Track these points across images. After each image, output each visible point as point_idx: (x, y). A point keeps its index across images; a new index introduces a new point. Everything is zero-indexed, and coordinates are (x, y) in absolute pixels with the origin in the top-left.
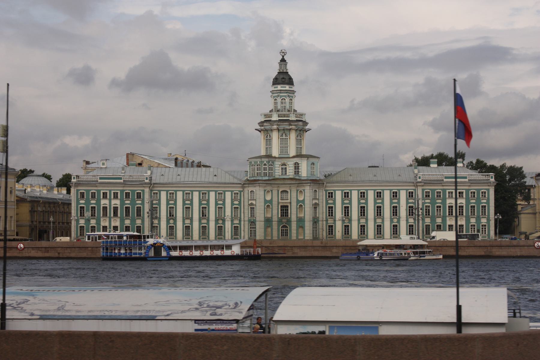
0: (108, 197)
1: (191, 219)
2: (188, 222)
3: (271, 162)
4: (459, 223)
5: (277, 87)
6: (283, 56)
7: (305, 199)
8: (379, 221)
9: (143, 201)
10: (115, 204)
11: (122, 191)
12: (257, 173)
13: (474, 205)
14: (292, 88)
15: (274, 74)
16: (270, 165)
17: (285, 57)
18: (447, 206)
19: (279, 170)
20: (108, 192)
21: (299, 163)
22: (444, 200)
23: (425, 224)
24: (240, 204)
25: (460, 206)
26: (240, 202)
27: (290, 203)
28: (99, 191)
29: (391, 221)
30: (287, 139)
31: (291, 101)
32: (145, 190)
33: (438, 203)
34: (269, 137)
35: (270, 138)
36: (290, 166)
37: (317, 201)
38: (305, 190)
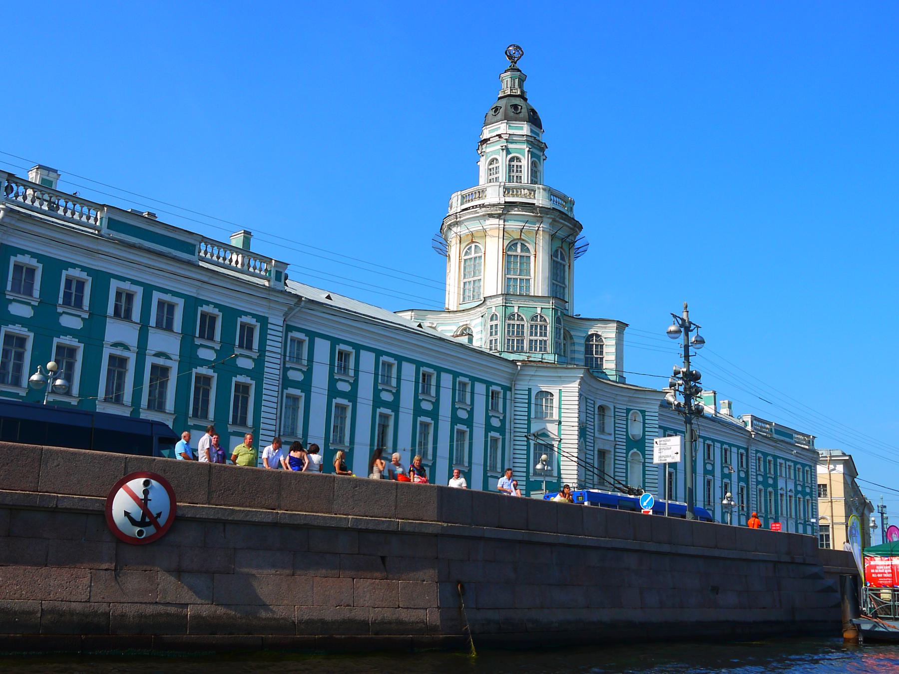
0: (136, 315)
5: (522, 128)
7: (647, 437)
9: (260, 362)
10: (159, 355)
11: (192, 303)
12: (531, 341)
20: (139, 291)
21: (604, 335)
22: (775, 480)
24: (502, 430)
26: (503, 421)
28: (101, 279)
30: (564, 266)
32: (270, 321)
33: (770, 485)
34: (519, 250)
35: (523, 254)
36: (576, 340)
38: (647, 414)
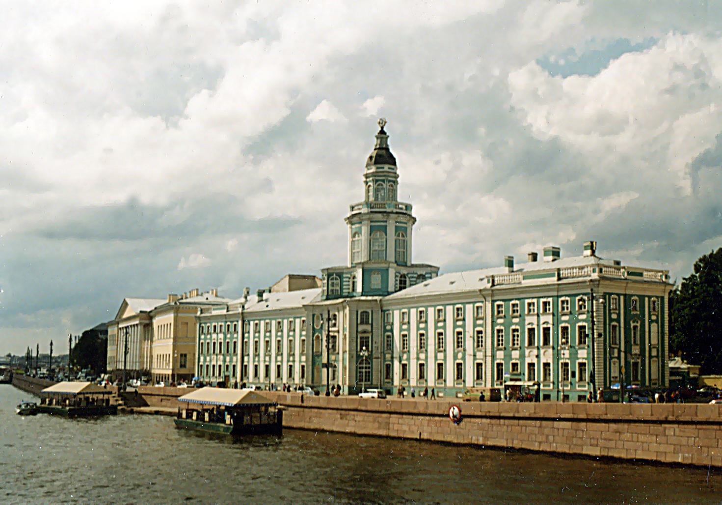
1: (270, 356)
2: (267, 358)
3: (335, 275)
4: (543, 360)
6: (382, 128)
8: (440, 356)
10: (220, 339)
13: (567, 325)
14: (383, 168)
15: (372, 152)
16: (331, 279)
17: (385, 129)
18: (527, 327)
19: (349, 285)
23: (511, 362)
25: (545, 329)
27: (338, 332)
29: (455, 357)
31: (380, 187)
33: (513, 324)
37: (368, 328)
